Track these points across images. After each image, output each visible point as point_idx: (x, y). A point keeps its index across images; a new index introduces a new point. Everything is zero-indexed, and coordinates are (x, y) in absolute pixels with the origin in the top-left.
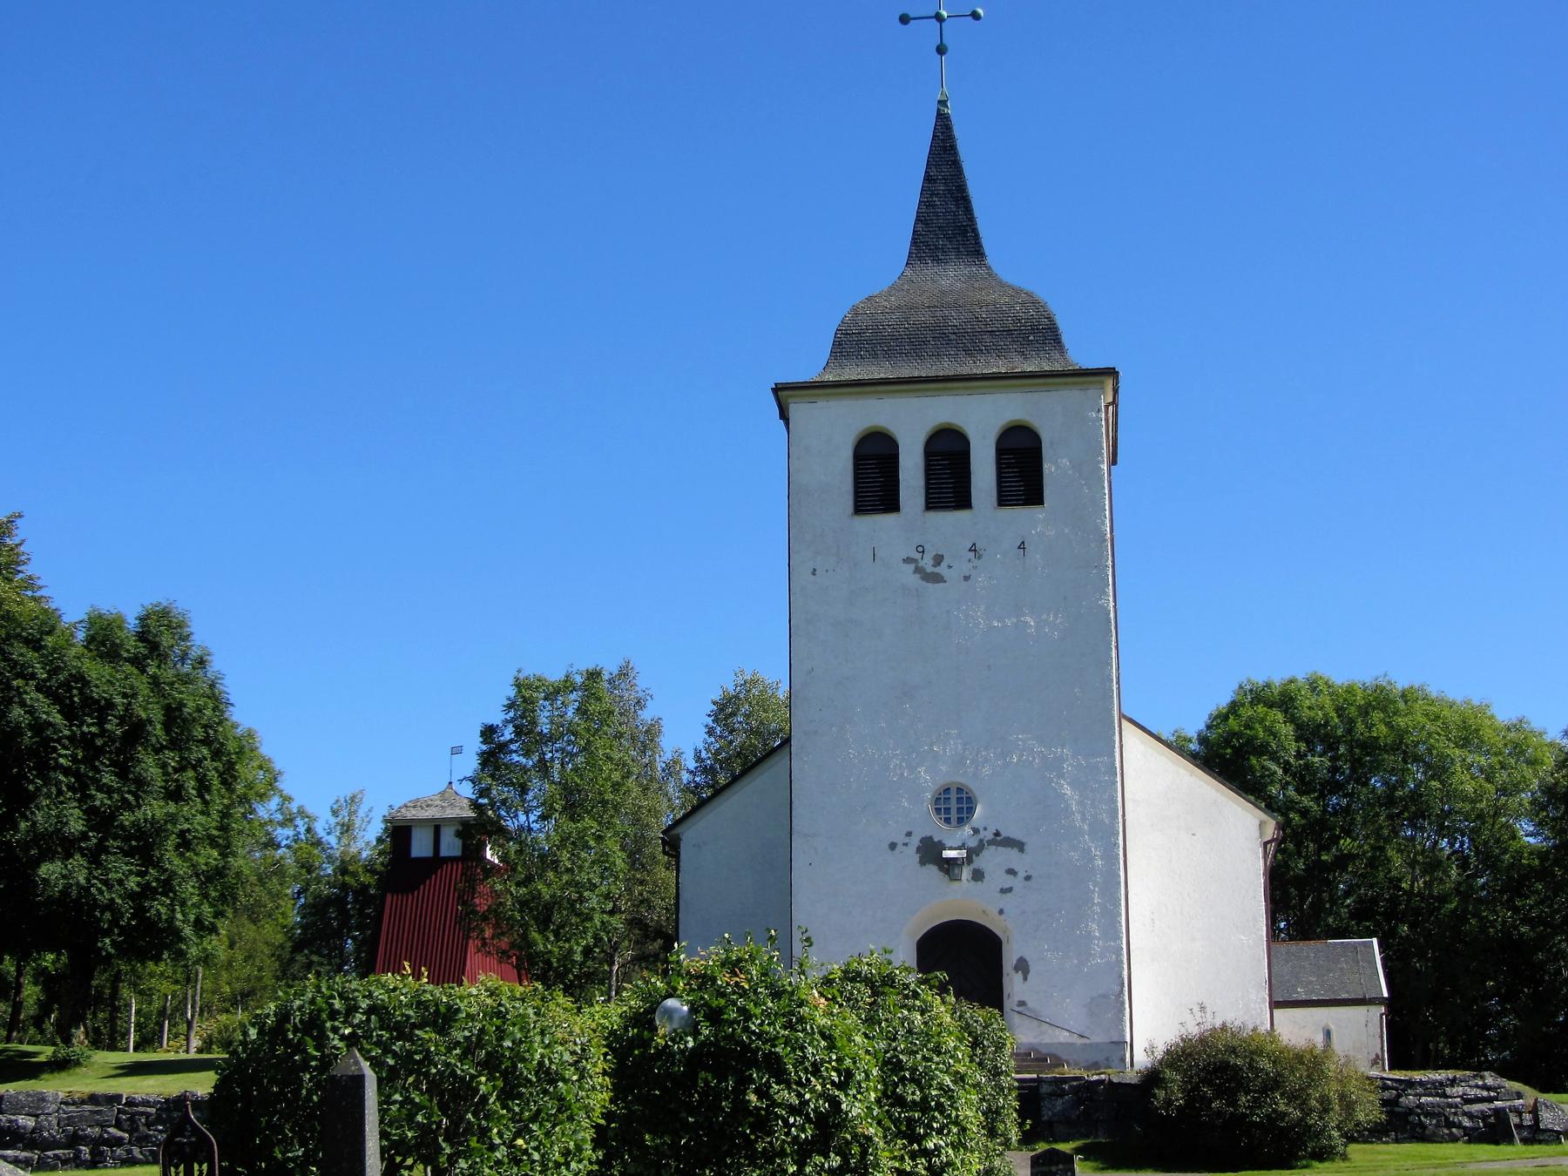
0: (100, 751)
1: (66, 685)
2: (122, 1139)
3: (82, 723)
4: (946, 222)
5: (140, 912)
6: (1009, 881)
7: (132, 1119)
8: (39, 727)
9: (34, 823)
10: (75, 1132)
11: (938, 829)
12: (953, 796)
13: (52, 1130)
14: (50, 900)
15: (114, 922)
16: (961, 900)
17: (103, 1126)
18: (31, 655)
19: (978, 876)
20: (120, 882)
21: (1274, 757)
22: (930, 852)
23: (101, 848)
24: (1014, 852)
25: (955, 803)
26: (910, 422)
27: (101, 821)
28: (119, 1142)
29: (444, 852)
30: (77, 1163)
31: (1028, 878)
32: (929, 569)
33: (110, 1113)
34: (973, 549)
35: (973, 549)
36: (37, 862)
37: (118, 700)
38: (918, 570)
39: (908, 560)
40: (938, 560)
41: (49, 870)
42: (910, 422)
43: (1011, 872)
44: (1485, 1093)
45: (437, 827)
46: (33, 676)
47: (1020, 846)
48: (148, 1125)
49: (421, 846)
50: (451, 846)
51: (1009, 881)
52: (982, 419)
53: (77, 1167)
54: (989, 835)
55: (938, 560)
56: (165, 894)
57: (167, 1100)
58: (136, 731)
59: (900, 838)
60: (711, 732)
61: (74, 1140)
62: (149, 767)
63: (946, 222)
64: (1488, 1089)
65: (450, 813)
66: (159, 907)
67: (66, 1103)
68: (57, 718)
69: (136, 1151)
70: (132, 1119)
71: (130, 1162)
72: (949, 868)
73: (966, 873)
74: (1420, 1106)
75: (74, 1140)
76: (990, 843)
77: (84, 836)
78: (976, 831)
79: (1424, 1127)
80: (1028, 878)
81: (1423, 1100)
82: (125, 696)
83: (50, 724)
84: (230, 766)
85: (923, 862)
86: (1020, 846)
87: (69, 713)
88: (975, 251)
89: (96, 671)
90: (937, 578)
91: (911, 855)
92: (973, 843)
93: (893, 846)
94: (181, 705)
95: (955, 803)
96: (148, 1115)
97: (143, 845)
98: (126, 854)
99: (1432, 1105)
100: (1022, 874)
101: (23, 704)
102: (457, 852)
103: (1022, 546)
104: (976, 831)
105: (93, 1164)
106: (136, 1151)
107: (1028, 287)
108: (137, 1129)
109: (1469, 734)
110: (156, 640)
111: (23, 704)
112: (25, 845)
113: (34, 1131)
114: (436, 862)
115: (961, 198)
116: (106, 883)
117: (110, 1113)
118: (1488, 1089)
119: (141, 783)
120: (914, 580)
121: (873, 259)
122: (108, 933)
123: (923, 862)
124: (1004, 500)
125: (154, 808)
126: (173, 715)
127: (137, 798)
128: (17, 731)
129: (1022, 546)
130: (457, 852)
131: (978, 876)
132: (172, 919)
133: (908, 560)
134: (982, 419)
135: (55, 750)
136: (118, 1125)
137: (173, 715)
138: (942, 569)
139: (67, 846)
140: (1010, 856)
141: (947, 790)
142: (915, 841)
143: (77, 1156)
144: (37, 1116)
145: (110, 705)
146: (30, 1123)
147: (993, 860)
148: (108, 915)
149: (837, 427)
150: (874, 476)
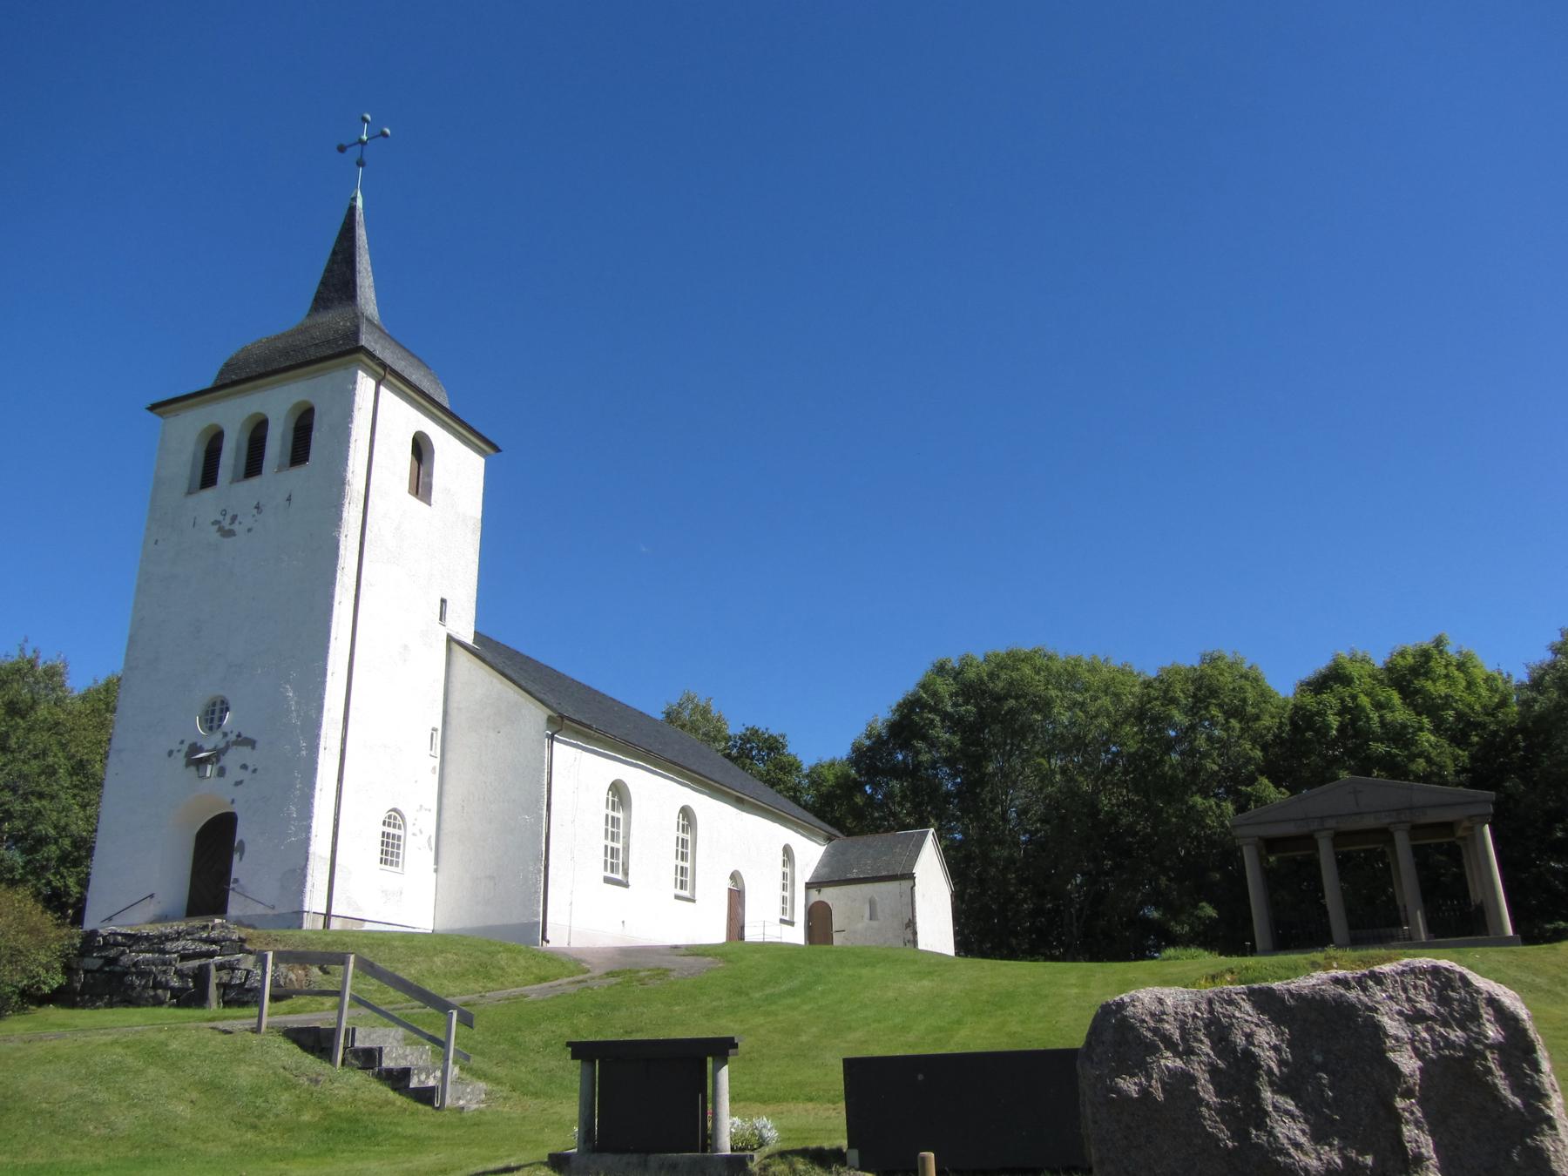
16: (212, 794)
19: (221, 772)
21: (933, 710)
24: (246, 750)
25: (214, 713)
32: (227, 527)
34: (257, 507)
38: (221, 529)
40: (234, 518)
43: (244, 767)
44: (205, 947)
47: (251, 743)
54: (232, 737)
55: (234, 518)
59: (175, 746)
64: (214, 942)
74: (135, 964)
76: (236, 743)
78: (225, 735)
79: (132, 986)
80: (255, 771)
81: (141, 956)
85: (188, 764)
86: (251, 743)
90: (229, 533)
91: (180, 759)
92: (222, 745)
93: (170, 753)
95: (214, 713)
99: (148, 962)
100: (251, 768)
103: (289, 499)
104: (225, 735)
109: (1069, 678)
118: (214, 942)
133: (216, 522)
138: (236, 527)
141: (214, 704)
142: (185, 748)
147: (231, 760)
149: (189, 427)
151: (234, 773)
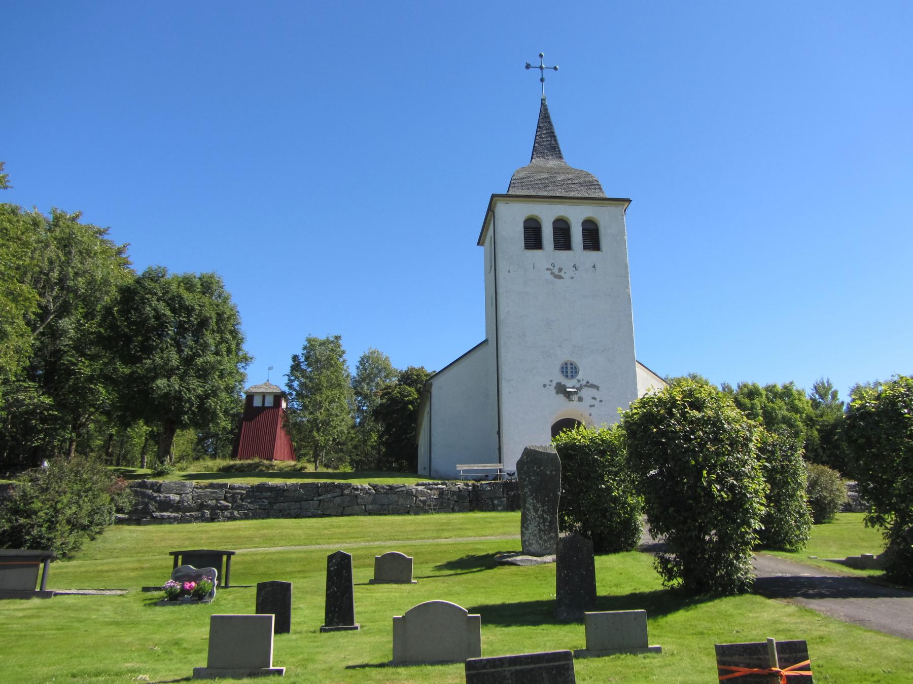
0: (186, 330)
1: (173, 299)
2: (227, 506)
3: (180, 315)
4: (547, 141)
5: (201, 406)
6: (593, 402)
7: (234, 496)
8: (158, 316)
9: (154, 360)
10: (202, 503)
11: (564, 381)
12: (569, 366)
13: (189, 499)
14: (160, 397)
15: (190, 409)
17: (217, 500)
18: (153, 285)
20: (194, 390)
22: (561, 389)
23: (186, 373)
24: (595, 390)
25: (569, 370)
26: (547, 215)
27: (188, 362)
28: (226, 508)
29: (266, 405)
30: (203, 519)
31: (601, 401)
32: (557, 273)
33: (221, 493)
35: (574, 266)
36: (154, 379)
37: (197, 307)
38: (552, 273)
39: (548, 269)
40: (560, 270)
41: (161, 382)
42: (547, 215)
43: (594, 398)
45: (264, 396)
46: (156, 294)
47: (597, 388)
48: (242, 500)
49: (257, 403)
50: (269, 402)
51: (593, 402)
52: (576, 216)
53: (203, 521)
54: (584, 383)
55: (560, 270)
56: (214, 397)
57: (252, 487)
58: (203, 323)
59: (548, 383)
60: (358, 368)
61: (201, 507)
62: (210, 339)
63: (547, 141)
65: (269, 390)
66: (211, 402)
67: (197, 488)
68: (168, 313)
69: (236, 513)
70: (234, 496)
71: (232, 518)
72: (568, 395)
73: (575, 398)
75: (201, 507)
76: (585, 386)
77: (178, 368)
78: (579, 381)
80: (601, 401)
82: (200, 306)
83: (164, 315)
84: (238, 344)
85: (557, 393)
86: (597, 388)
87: (173, 310)
88: (560, 157)
89: (186, 295)
90: (560, 277)
92: (578, 385)
93: (545, 386)
94: (224, 313)
95: (569, 370)
96: (242, 494)
97: (204, 374)
98: (197, 377)
100: (598, 400)
101: (150, 306)
102: (271, 405)
105: (212, 519)
106: (236, 513)
107: (585, 169)
108: (236, 502)
110: (207, 286)
111: (150, 306)
112: (149, 370)
113: (179, 502)
114: (263, 408)
115: (552, 135)
116: (188, 389)
117: (221, 493)
119: (205, 346)
120: (551, 277)
121: (516, 154)
122: (186, 413)
123: (557, 393)
124: (586, 247)
125: (211, 358)
126: (220, 316)
127: (203, 352)
128: (147, 319)
129: (594, 267)
130: (271, 405)
131: (580, 399)
132: (216, 408)
133: (548, 269)
134: (576, 216)
135: (167, 327)
136: (225, 499)
137: (220, 316)
138: (562, 274)
139: (169, 373)
140: (593, 392)
142: (554, 384)
143: (203, 516)
144: (181, 494)
145: (193, 309)
146: (177, 498)
147: (586, 393)
148: (187, 405)
150: (532, 236)
151: (588, 401)
